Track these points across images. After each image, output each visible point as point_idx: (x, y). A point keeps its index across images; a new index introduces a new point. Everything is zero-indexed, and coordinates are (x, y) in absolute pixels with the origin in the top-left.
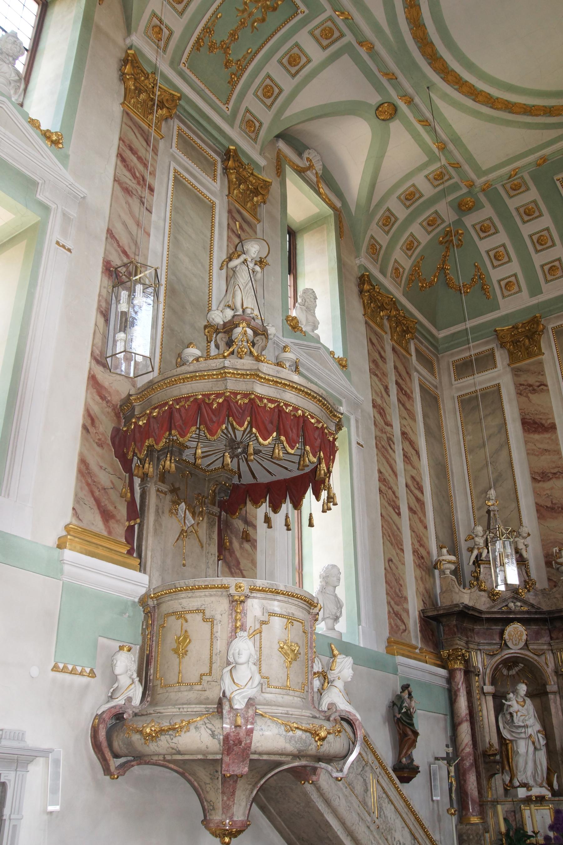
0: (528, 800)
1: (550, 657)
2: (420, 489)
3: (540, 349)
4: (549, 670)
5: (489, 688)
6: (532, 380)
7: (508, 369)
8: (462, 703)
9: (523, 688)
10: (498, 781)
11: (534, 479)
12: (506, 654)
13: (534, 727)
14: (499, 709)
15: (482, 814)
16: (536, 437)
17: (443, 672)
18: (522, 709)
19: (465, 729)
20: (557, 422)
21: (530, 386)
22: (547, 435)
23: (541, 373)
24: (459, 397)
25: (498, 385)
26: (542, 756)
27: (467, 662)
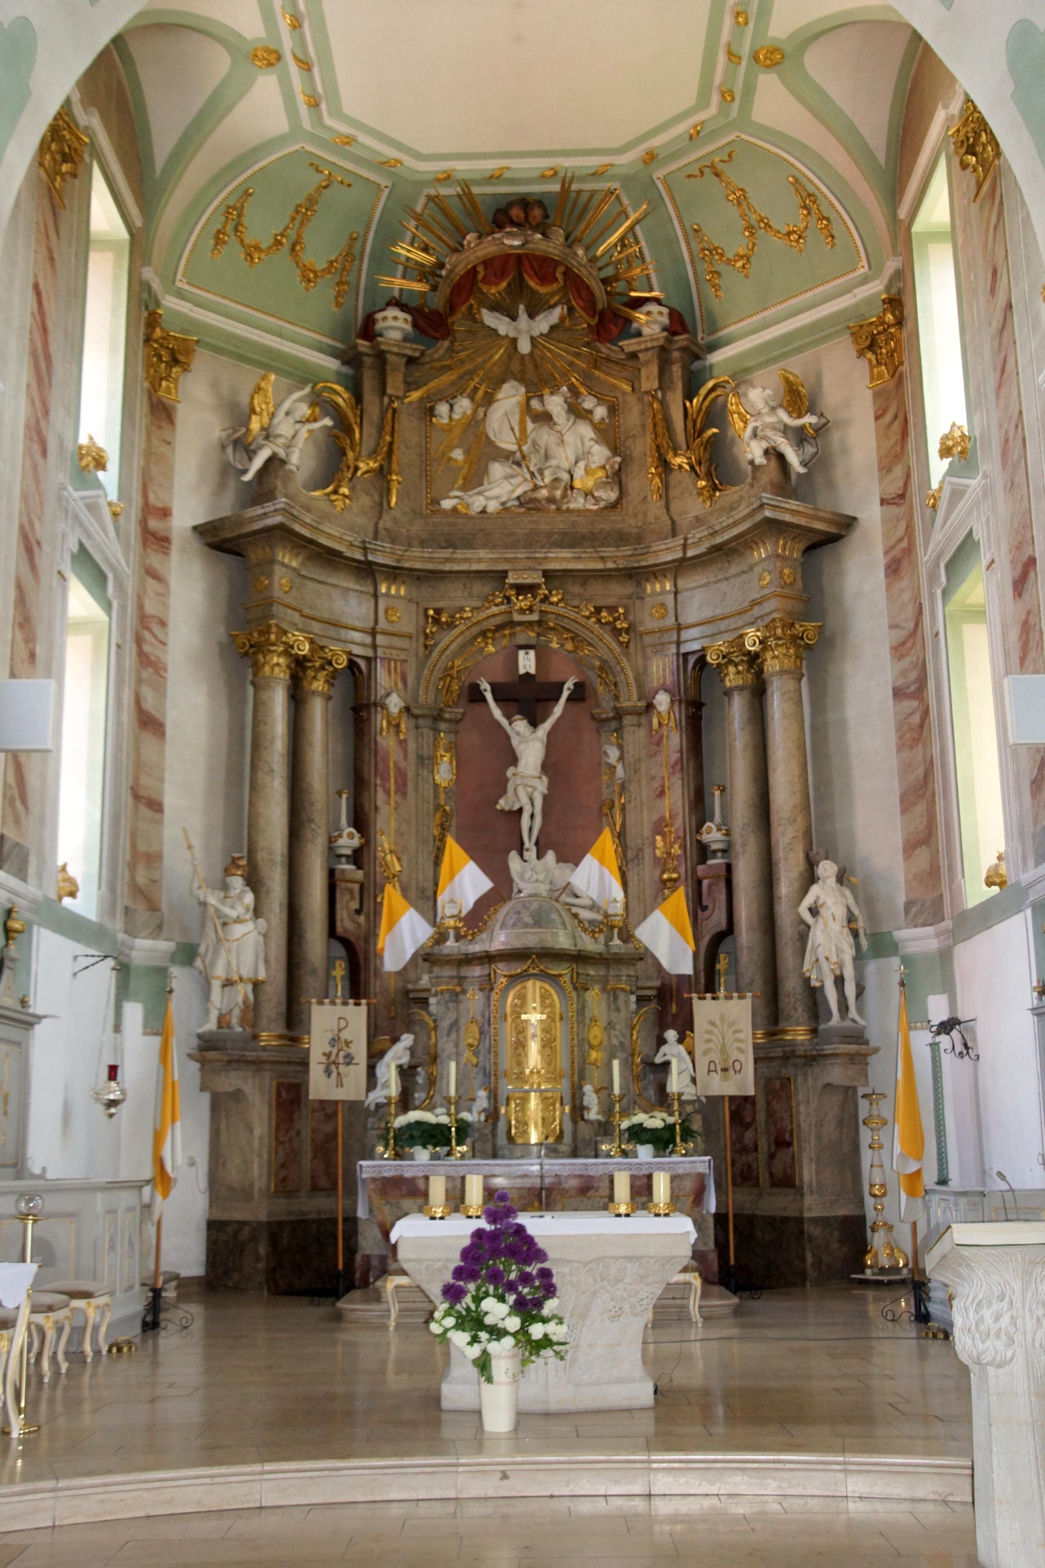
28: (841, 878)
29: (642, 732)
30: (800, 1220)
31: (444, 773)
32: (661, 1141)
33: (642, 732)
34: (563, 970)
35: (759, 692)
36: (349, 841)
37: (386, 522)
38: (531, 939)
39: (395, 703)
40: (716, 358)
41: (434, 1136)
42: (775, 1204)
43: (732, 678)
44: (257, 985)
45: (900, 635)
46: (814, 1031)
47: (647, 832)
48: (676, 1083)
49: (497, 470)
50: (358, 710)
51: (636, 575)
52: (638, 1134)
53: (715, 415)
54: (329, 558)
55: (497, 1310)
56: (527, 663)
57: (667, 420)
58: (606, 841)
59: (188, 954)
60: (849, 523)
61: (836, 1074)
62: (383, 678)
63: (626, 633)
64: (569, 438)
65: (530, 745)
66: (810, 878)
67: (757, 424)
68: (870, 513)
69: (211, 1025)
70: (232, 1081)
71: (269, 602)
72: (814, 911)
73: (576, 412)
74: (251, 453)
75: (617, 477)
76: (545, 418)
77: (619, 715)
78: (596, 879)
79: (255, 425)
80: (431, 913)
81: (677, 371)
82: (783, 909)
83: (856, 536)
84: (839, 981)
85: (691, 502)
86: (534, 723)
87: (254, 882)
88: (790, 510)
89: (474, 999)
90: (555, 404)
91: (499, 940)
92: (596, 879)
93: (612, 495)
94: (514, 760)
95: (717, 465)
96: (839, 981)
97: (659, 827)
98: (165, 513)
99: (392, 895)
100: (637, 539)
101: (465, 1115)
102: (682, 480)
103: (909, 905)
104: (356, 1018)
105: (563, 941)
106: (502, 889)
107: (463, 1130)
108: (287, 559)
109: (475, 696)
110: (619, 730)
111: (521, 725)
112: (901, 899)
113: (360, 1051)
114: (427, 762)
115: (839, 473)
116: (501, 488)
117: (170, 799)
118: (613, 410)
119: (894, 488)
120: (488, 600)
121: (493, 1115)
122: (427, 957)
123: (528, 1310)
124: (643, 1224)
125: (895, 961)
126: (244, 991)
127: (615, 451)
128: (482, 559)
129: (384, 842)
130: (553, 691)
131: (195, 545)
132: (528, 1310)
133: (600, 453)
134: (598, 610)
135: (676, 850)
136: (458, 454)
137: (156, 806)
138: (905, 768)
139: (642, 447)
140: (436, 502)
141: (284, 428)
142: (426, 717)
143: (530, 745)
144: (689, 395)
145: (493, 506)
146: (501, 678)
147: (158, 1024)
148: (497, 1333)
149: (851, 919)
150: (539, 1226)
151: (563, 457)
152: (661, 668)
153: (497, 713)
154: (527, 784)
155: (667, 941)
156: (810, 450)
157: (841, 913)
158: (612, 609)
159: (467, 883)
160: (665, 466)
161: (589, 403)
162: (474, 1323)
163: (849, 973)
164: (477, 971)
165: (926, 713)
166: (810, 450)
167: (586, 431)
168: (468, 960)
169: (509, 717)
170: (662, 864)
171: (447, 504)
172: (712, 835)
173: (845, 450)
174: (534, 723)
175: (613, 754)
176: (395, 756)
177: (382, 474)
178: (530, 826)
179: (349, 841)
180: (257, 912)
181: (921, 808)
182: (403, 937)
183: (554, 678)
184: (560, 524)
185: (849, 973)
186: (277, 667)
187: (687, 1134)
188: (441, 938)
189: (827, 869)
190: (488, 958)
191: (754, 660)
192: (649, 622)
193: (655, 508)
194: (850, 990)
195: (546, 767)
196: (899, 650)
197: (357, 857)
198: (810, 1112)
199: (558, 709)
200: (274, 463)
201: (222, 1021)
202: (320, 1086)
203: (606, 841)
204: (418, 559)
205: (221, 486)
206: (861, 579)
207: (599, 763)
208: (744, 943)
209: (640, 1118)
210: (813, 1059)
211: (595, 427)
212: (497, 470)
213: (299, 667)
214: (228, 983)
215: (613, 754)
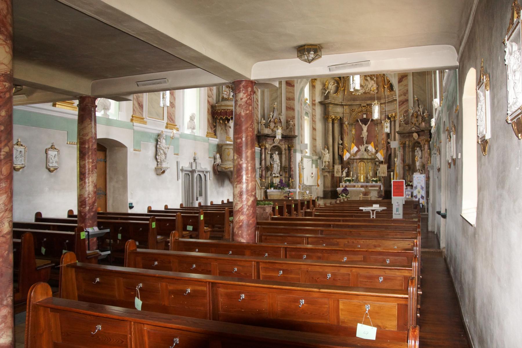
0: (275, 177)
1: (284, 146)
2: (258, 101)
4: (283, 149)
5: (269, 152)
8: (263, 156)
9: (277, 153)
10: (269, 173)
11: (287, 99)
12: (274, 145)
14: (271, 157)
15: (265, 179)
16: (289, 87)
17: (260, 149)
18: (276, 157)
19: (263, 162)
26: (279, 168)
27: (265, 147)
31: (353, 132)
32: (376, 181)
34: (366, 161)
36: (341, 142)
37: (345, 97)
38: (362, 157)
39: (346, 123)
41: (349, 181)
44: (329, 162)
50: (341, 124)
52: (373, 181)
54: (337, 105)
55: (344, 195)
56: (365, 116)
58: (372, 143)
59: (320, 158)
62: (345, 119)
65: (365, 128)
69: (323, 167)
70: (326, 174)
71: (329, 112)
74: (326, 91)
75: (378, 89)
76: (367, 80)
77: (377, 124)
78: (371, 148)
79: (326, 86)
80: (350, 153)
85: (387, 92)
86: (366, 125)
87: (328, 149)
89: (355, 164)
91: (358, 157)
92: (371, 148)
94: (362, 130)
98: (315, 101)
99: (345, 151)
102: (386, 89)
104: (340, 167)
105: (366, 157)
106: (359, 150)
107: (353, 180)
108: (331, 106)
109: (358, 121)
111: (363, 126)
113: (341, 171)
114: (351, 131)
117: (317, 138)
120: (359, 107)
121: (357, 178)
122: (349, 159)
123: (347, 195)
124: (358, 189)
126: (327, 163)
127: (377, 84)
128: (358, 103)
129: (345, 142)
130: (369, 120)
131: (319, 104)
132: (347, 195)
133: (375, 85)
137: (315, 140)
139: (381, 84)
141: (330, 87)
142: (350, 124)
143: (365, 128)
146: (361, 118)
147: (316, 167)
150: (347, 188)
151: (370, 86)
154: (365, 134)
155: (380, 156)
159: (355, 149)
160: (384, 87)
164: (355, 161)
168: (354, 159)
170: (383, 144)
175: (377, 129)
176: (347, 130)
177: (344, 90)
178: (365, 140)
179: (341, 142)
180: (329, 153)
182: (346, 156)
184: (369, 96)
186: (330, 121)
187: (380, 180)
188: (351, 156)
190: (357, 159)
195: (368, 131)
197: (342, 144)
199: (369, 123)
200: (329, 92)
201: (325, 167)
202: (336, 175)
203: (372, 143)
204: (349, 103)
205: (322, 95)
207: (375, 130)
213: (333, 120)
214: (325, 162)
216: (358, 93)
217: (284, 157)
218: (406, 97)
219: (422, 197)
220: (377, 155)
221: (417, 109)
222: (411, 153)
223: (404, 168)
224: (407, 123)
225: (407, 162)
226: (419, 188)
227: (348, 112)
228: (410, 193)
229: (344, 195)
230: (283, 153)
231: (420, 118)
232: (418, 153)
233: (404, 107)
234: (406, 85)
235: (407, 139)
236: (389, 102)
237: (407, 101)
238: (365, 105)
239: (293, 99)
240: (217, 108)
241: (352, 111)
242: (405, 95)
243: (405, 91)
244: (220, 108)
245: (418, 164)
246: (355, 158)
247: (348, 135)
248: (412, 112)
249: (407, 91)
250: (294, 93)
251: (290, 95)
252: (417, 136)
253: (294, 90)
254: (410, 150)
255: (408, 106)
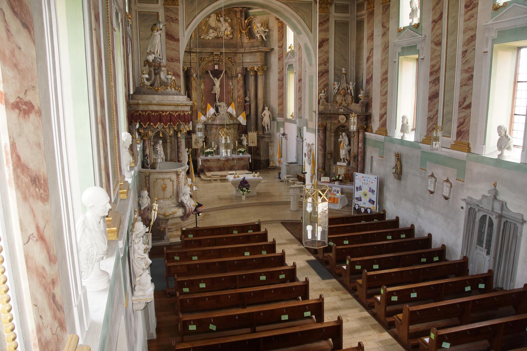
3: (178, 2)
6: (173, 16)
7: (163, 7)
9: (161, 142)
13: (162, 153)
16: (171, 42)
18: (160, 148)
20: (180, 38)
21: (172, 18)
22: (176, 43)
23: (177, 14)
24: (139, 12)
25: (158, 13)
28: (268, 110)
29: (236, 80)
30: (260, 160)
31: (202, 87)
32: (243, 153)
33: (236, 80)
35: (256, 76)
39: (194, 75)
40: (250, 11)
41: (211, 153)
42: (257, 158)
43: (252, 73)
45: (280, 70)
46: (263, 133)
47: (236, 97)
48: (245, 143)
49: (211, 31)
51: (236, 53)
52: (240, 152)
53: (250, 24)
55: (244, 189)
56: (216, 67)
57: (241, 23)
60: (272, 49)
61: (266, 140)
62: (192, 71)
63: (234, 63)
64: (224, 26)
65: (217, 82)
66: (264, 109)
67: (258, 29)
68: (276, 48)
72: (264, 115)
73: (226, 21)
75: (232, 33)
76: (219, 21)
77: (232, 77)
78: (232, 110)
81: (243, 14)
82: (259, 114)
83: (273, 51)
84: (268, 126)
85: (246, 40)
86: (218, 79)
88: (264, 49)
89: (214, 131)
90: (222, 19)
91: (218, 122)
93: (231, 36)
94: (215, 85)
95: (251, 34)
96: (268, 126)
97: (239, 97)
100: (235, 46)
101: (215, 149)
103: (278, 114)
109: (207, 72)
110: (232, 79)
111: (216, 79)
112: (277, 113)
114: (200, 85)
115: (271, 39)
116: (212, 35)
118: (231, 20)
119: (280, 45)
125: (276, 122)
127: (232, 28)
128: (210, 50)
132: (247, 189)
133: (229, 29)
134: (229, 58)
135: (241, 101)
136: (204, 27)
138: (279, 92)
139: (237, 27)
140: (200, 37)
143: (217, 82)
144: (245, 19)
145: (210, 38)
146: (212, 69)
148: (245, 191)
149: (270, 116)
151: (223, 29)
152: (239, 69)
153: (211, 76)
154: (217, 89)
156: (266, 34)
157: (268, 115)
158: (231, 58)
161: (227, 18)
162: (242, 190)
163: (269, 124)
165: (283, 85)
166: (266, 34)
167: (227, 24)
168: (213, 124)
169: (214, 77)
170: (239, 103)
171: (202, 37)
172: (247, 99)
173: (272, 36)
174: (218, 79)
175: (231, 84)
181: (281, 99)
183: (221, 70)
185: (269, 124)
189: (266, 108)
190: (217, 125)
191: (256, 72)
192: (238, 61)
193: (239, 40)
194: (269, 127)
195: (221, 86)
196: (280, 73)
198: (262, 145)
206: (274, 59)
208: (255, 123)
209: (240, 149)
210: (263, 137)
211: (229, 24)
212: (211, 31)
215: (231, 84)
216: (208, 38)
217: (169, 145)
218: (326, 67)
219: (371, 201)
220: (238, 118)
221: (344, 85)
222: (333, 139)
223: (324, 156)
224: (327, 99)
225: (328, 149)
226: (365, 189)
227: (195, 61)
228: (339, 189)
229: (244, 189)
230: (168, 141)
231: (349, 98)
232: (344, 139)
233: (324, 79)
234: (327, 52)
235: (329, 121)
236: (247, 52)
237: (327, 71)
238: (219, 53)
239: (178, 61)
240: (141, 108)
241: (201, 59)
242: (325, 65)
243: (325, 59)
244: (146, 108)
245: (343, 153)
246: (215, 123)
247: (196, 90)
248: (337, 87)
249: (328, 59)
250: (179, 51)
251: (173, 54)
252: (345, 119)
253: (178, 47)
254: (333, 134)
255: (328, 79)
